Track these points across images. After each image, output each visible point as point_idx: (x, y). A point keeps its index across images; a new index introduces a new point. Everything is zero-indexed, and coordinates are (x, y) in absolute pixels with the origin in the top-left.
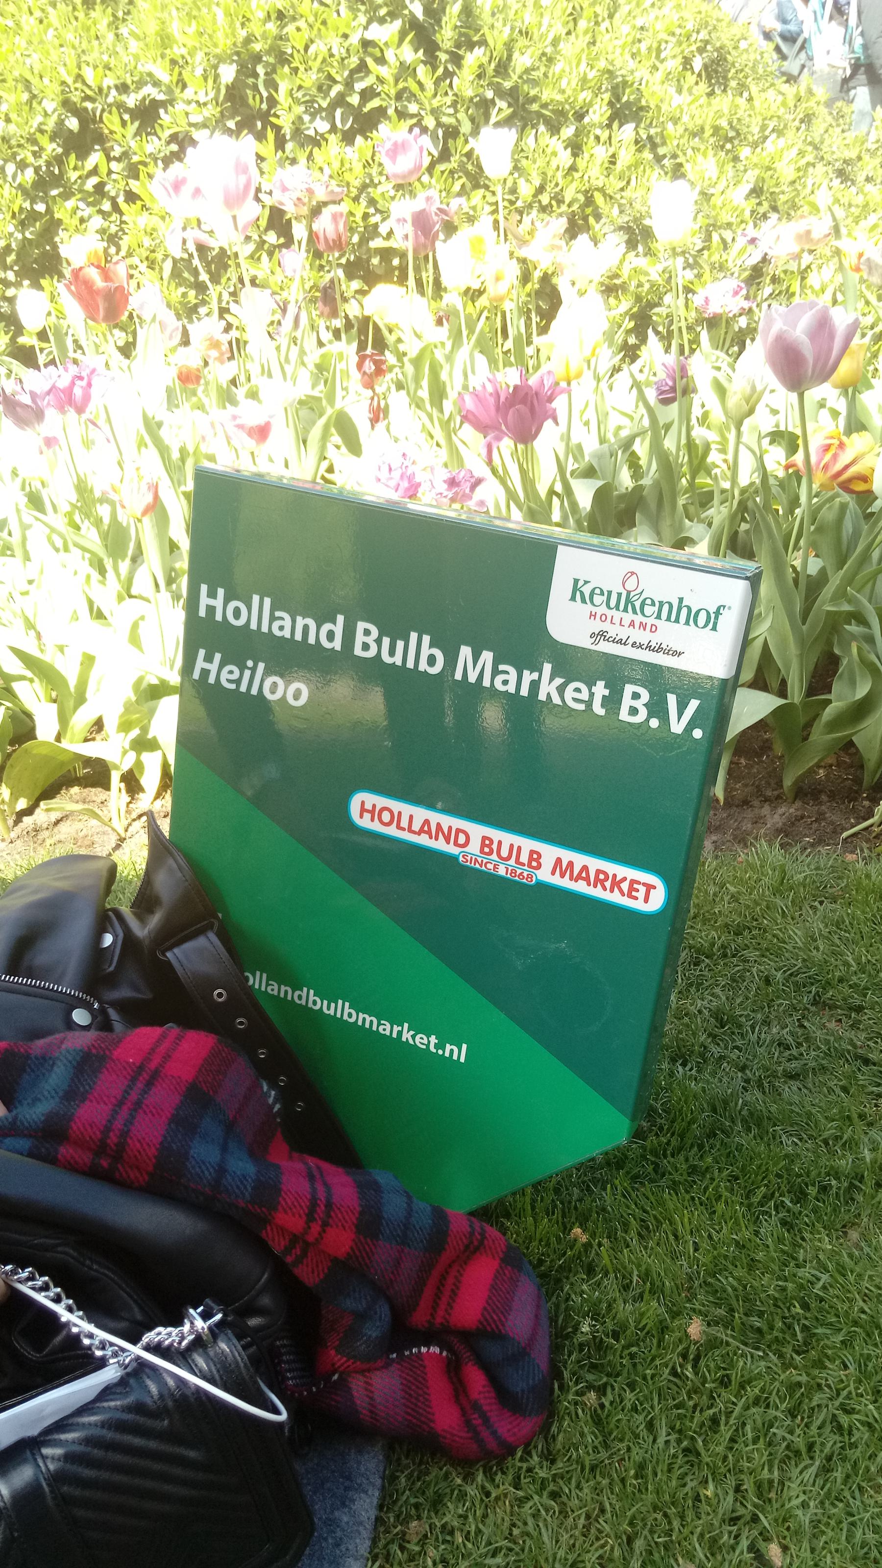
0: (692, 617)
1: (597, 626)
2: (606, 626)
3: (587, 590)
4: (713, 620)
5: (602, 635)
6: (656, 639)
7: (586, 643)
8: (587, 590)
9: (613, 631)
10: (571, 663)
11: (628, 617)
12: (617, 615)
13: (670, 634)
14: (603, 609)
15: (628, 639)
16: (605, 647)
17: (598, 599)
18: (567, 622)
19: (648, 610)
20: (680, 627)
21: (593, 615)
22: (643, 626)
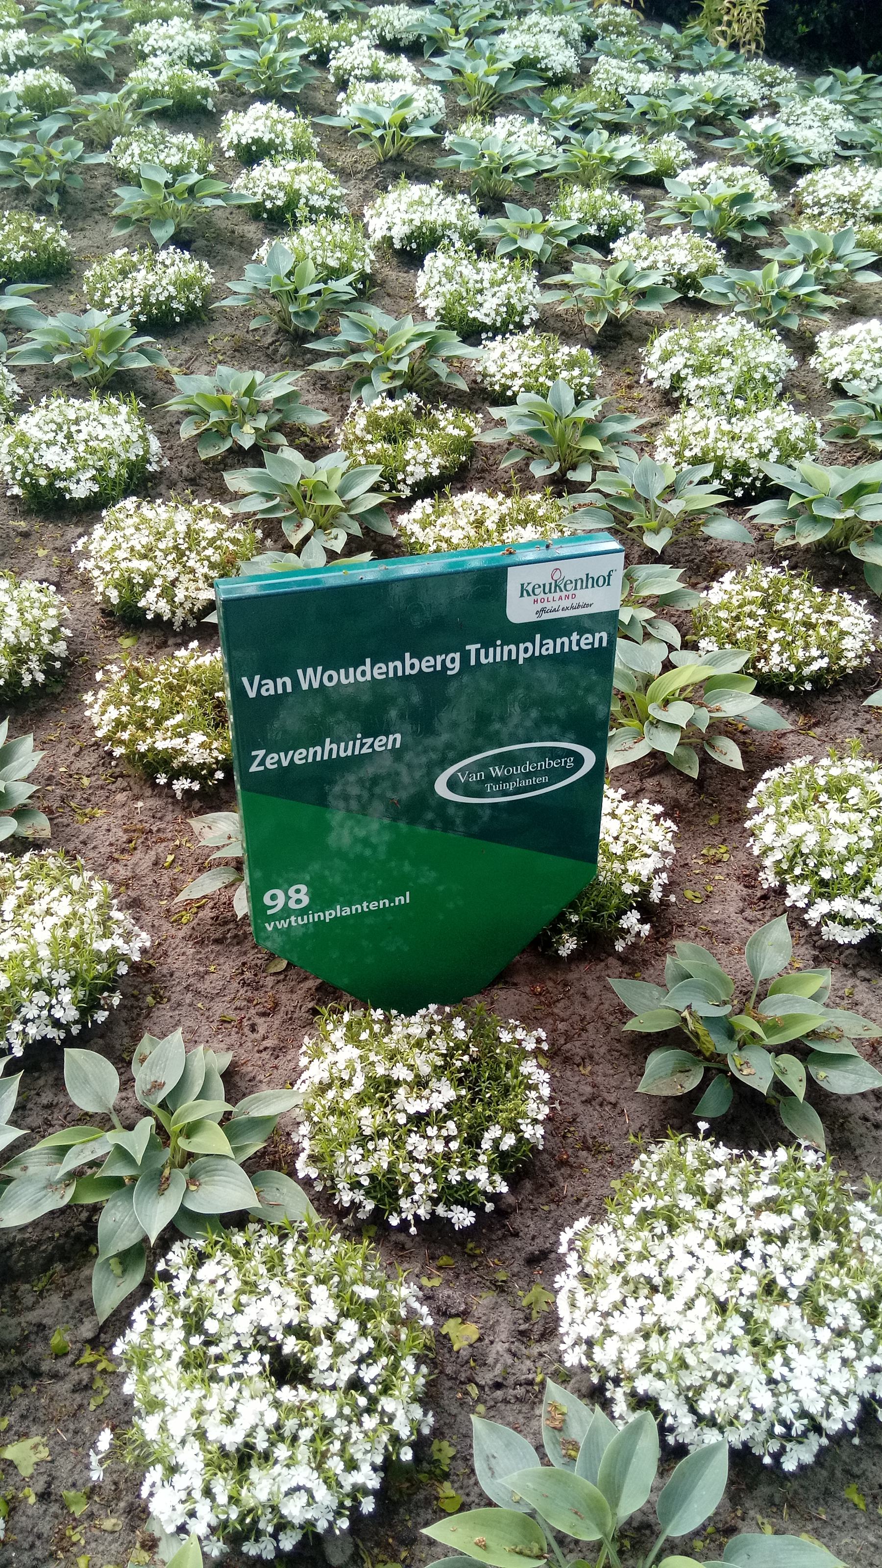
0: (595, 582)
1: (539, 606)
2: (545, 604)
3: (530, 589)
4: (607, 580)
5: (543, 610)
6: (575, 602)
7: (534, 618)
8: (530, 589)
9: (548, 606)
10: (526, 632)
11: (559, 594)
12: (550, 596)
13: (584, 595)
14: (542, 595)
15: (560, 607)
16: (545, 617)
17: (537, 591)
18: (520, 610)
19: (569, 587)
20: (590, 590)
21: (535, 601)
22: (567, 597)
